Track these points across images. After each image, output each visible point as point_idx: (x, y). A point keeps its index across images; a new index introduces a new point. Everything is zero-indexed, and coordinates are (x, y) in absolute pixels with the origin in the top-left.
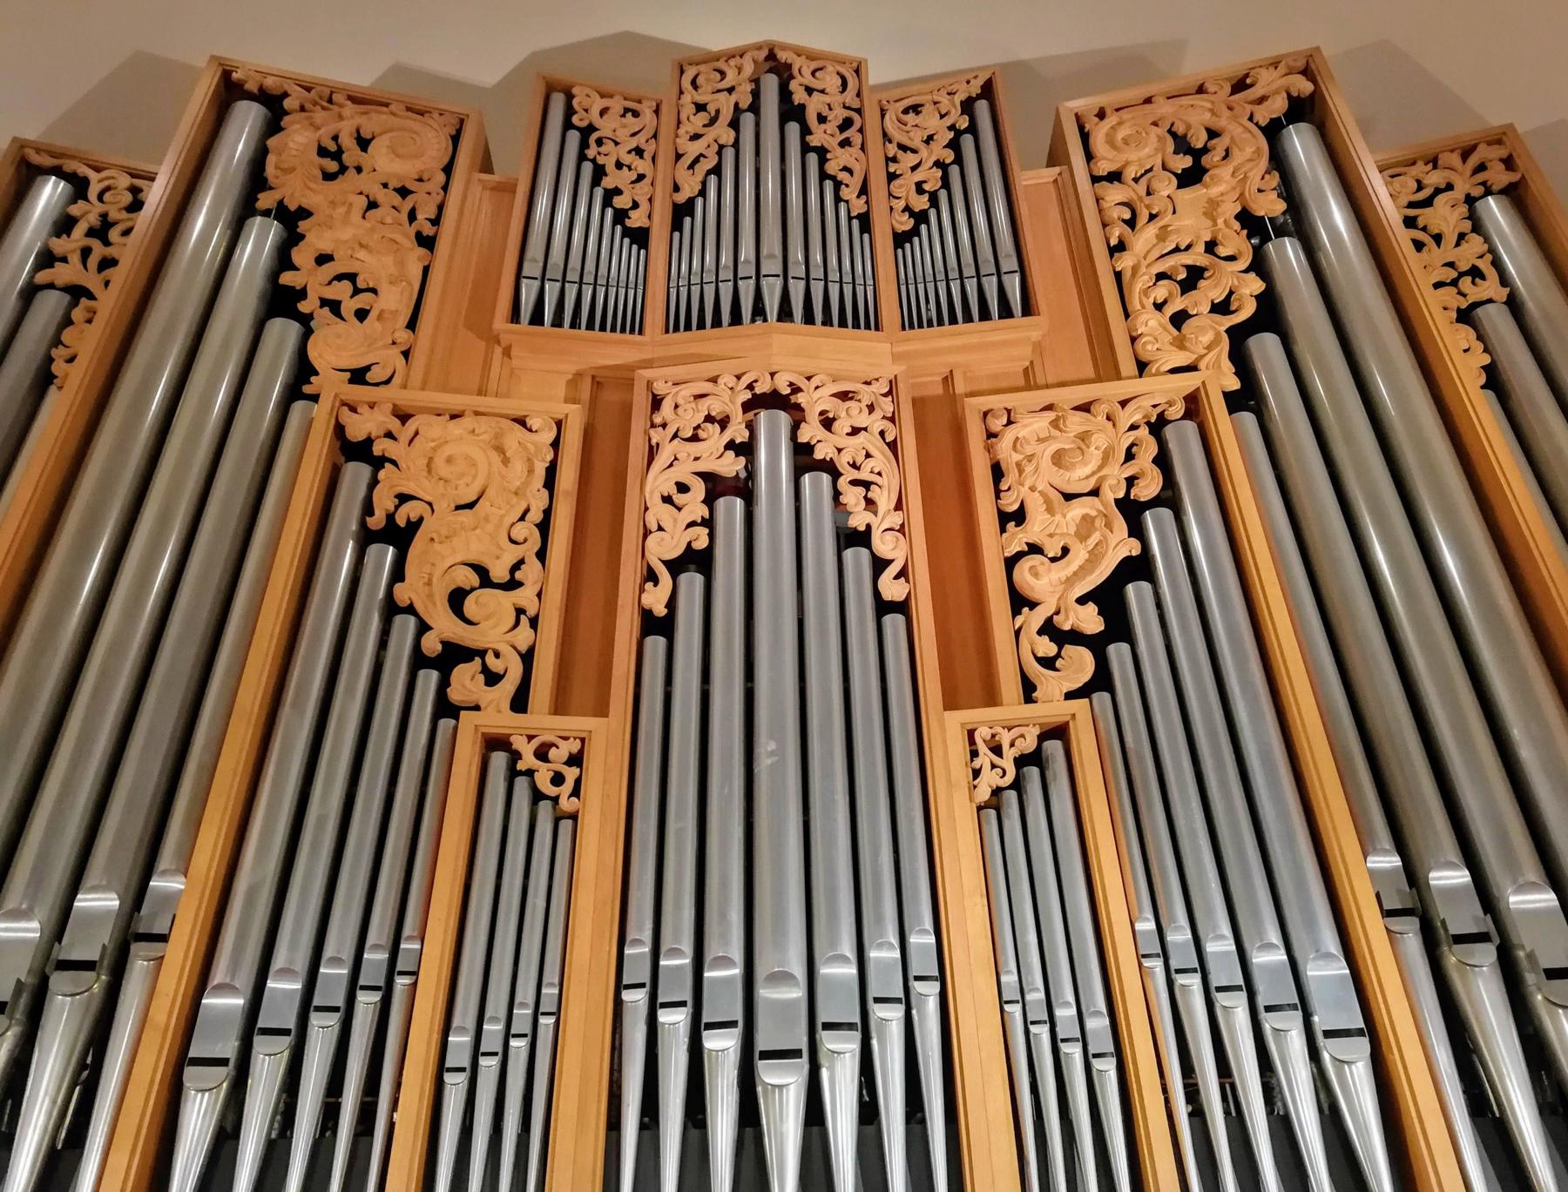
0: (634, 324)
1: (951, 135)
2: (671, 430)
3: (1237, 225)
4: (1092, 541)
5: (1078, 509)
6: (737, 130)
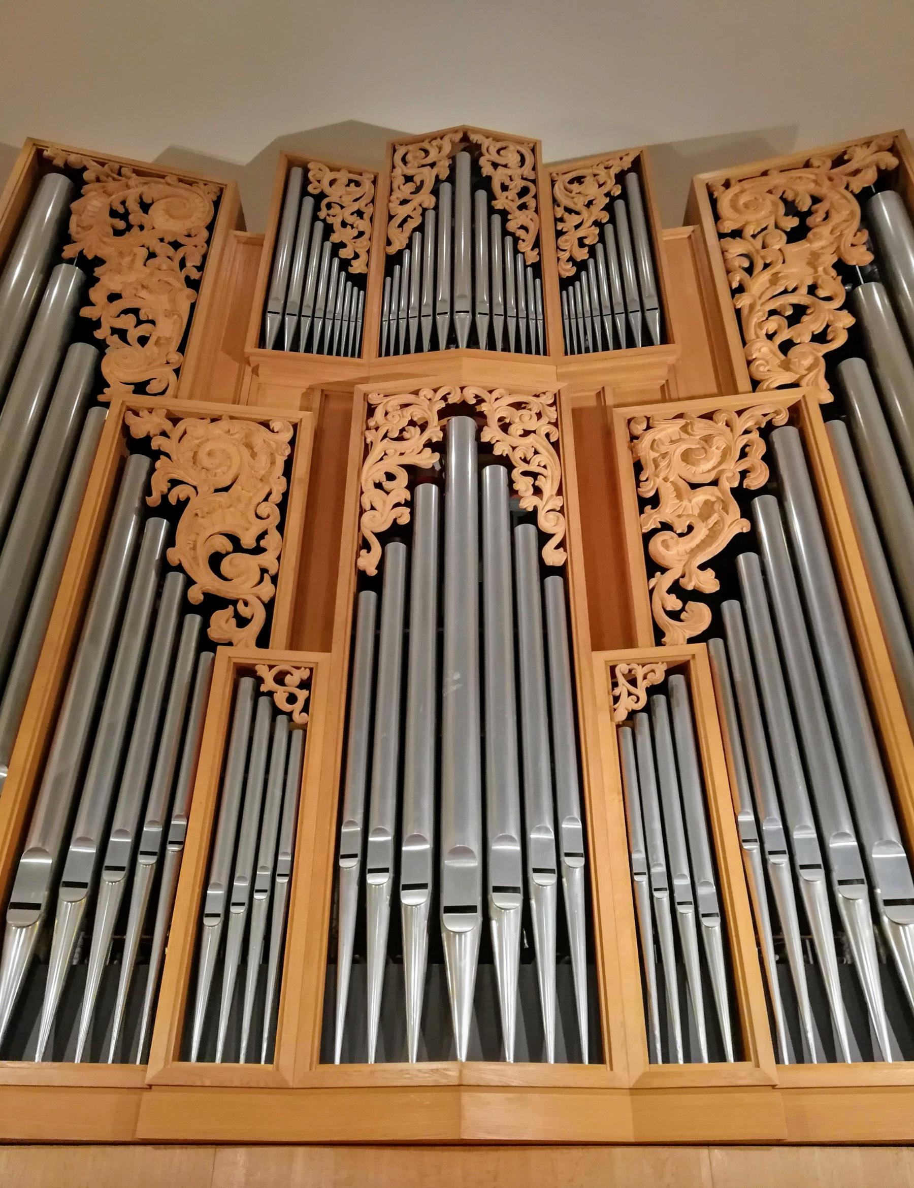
1: (607, 200)
2: (382, 432)
3: (834, 273)
4: (714, 518)
5: (701, 496)
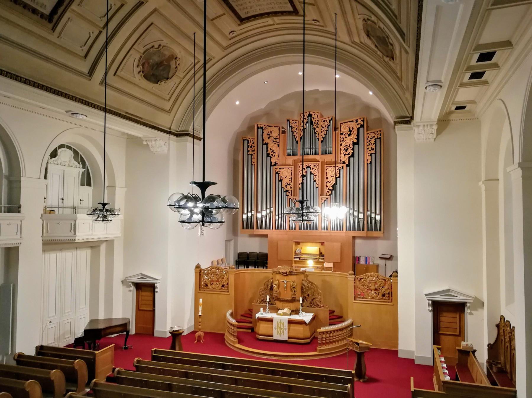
0: (297, 155)
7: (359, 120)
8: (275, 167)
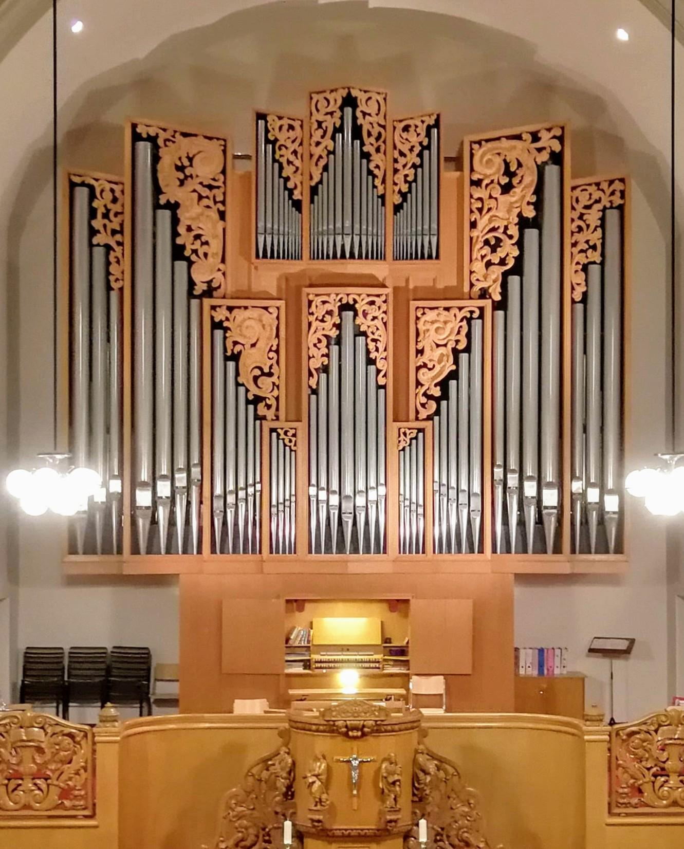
0: (299, 257)
4: (443, 364)
5: (442, 350)
6: (335, 142)
7: (545, 136)
8: (207, 302)
